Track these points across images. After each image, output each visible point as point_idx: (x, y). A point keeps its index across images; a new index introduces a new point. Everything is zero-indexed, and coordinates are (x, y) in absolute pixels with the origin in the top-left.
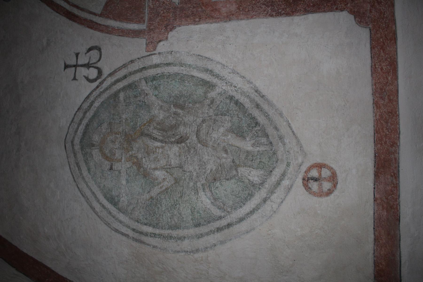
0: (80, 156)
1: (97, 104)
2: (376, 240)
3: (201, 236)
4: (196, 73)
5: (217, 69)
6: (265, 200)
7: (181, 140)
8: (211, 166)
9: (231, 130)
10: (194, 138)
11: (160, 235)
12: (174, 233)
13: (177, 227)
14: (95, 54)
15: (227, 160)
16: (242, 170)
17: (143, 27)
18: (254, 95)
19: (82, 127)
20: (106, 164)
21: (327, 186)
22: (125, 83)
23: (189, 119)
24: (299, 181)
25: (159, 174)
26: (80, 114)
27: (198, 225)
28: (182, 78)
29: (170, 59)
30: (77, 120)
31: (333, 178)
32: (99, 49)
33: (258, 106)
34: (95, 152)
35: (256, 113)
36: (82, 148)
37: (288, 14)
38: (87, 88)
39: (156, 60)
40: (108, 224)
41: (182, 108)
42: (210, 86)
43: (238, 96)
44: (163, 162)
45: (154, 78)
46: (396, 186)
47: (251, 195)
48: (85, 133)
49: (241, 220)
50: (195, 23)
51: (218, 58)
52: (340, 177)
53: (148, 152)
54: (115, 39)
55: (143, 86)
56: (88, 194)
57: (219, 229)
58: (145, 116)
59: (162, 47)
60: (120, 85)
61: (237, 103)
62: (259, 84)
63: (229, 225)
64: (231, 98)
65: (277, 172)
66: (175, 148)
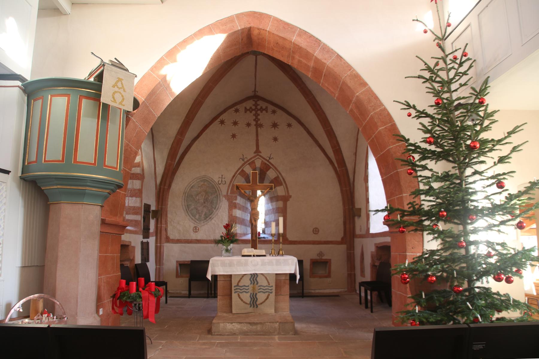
7: (204, 203)
8: (199, 209)
14: (224, 183)
15: (200, 212)
28: (217, 203)
31: (196, 232)
34: (202, 183)
39: (221, 197)
42: (215, 209)
53: (202, 195)
54: (227, 188)
59: (224, 199)
62: (215, 218)
66: (203, 201)
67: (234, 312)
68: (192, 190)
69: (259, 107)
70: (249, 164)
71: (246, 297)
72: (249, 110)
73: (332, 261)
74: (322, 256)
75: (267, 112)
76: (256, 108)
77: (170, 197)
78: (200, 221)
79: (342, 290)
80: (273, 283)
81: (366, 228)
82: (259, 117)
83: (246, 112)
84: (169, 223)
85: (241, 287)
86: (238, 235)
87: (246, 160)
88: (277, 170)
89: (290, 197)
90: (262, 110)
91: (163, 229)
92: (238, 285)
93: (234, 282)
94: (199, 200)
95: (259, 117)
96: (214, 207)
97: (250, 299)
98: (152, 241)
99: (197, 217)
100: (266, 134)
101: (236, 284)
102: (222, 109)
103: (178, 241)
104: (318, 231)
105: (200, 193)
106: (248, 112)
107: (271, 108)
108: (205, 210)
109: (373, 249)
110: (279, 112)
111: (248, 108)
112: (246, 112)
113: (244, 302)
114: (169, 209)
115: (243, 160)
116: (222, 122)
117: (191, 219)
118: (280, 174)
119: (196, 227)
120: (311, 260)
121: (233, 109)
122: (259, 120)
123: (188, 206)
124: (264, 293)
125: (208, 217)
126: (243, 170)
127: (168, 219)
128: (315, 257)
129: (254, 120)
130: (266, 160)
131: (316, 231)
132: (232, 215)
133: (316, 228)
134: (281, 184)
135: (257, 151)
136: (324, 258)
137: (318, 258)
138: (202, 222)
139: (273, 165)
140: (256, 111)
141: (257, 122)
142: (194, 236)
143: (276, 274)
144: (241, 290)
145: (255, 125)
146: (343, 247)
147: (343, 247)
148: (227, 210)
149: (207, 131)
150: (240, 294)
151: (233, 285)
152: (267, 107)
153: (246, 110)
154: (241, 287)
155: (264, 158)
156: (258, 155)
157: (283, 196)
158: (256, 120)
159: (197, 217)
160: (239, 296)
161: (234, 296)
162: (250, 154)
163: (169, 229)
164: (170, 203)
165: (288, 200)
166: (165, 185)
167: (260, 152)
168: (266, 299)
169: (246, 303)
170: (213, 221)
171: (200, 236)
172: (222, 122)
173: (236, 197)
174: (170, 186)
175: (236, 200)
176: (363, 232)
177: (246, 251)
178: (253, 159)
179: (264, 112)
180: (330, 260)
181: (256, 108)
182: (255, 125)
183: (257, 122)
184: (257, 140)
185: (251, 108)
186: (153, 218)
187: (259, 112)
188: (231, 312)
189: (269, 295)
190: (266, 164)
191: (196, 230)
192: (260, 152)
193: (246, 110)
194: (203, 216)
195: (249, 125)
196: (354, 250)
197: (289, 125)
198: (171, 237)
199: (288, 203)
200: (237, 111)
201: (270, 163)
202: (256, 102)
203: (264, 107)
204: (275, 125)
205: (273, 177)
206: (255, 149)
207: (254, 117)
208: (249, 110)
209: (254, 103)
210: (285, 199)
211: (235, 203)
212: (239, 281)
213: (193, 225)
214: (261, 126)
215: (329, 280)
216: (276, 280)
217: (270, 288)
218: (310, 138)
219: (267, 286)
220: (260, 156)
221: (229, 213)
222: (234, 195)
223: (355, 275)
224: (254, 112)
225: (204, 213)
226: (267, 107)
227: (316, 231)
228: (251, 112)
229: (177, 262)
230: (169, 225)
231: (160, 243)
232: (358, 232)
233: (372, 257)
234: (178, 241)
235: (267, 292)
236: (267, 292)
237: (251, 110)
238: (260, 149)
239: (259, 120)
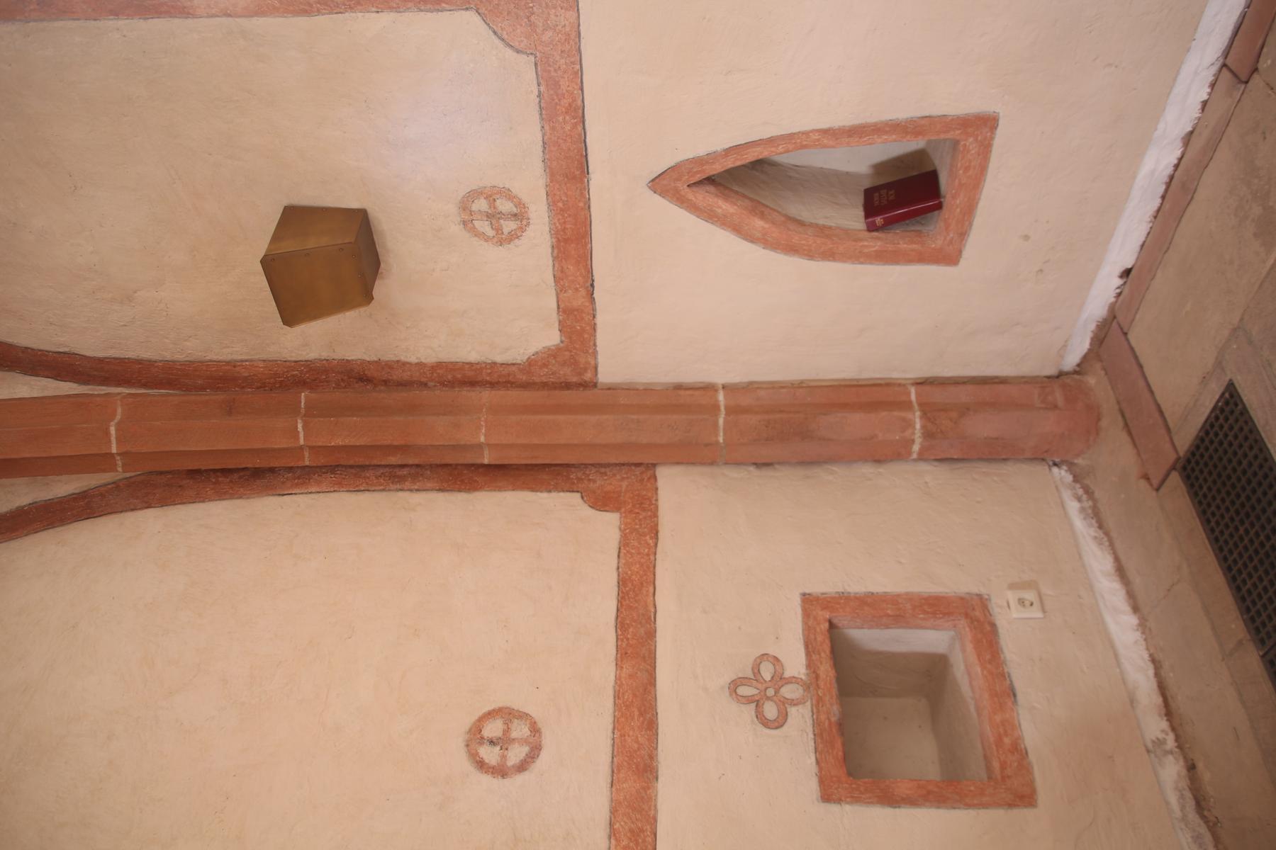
73: (826, 583)
74: (780, 680)
79: (1073, 506)
104: (507, 714)
120: (827, 796)
128: (794, 751)
131: (502, 742)
133: (475, 735)
136: (796, 664)
137: (801, 719)
146: (677, 490)
180: (809, 601)
215: (1012, 618)
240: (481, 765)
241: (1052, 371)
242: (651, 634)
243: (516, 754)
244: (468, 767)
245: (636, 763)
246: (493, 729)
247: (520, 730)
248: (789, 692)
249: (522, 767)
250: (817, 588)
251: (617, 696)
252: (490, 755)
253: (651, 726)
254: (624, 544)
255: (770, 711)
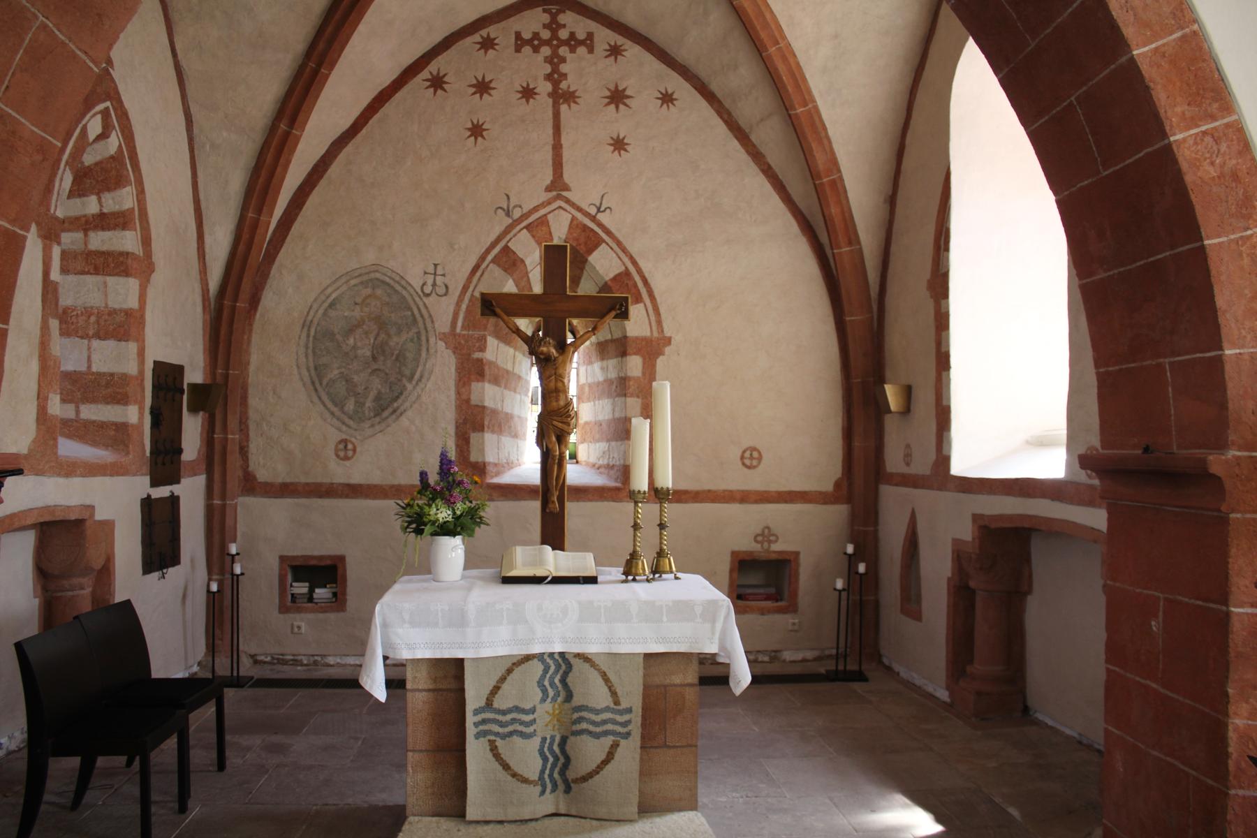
0: (365, 278)
1: (404, 293)
2: (307, 484)
3: (308, 370)
4: (420, 369)
5: (421, 385)
6: (332, 414)
7: (374, 358)
8: (356, 378)
9: (379, 393)
10: (376, 367)
11: (308, 340)
12: (310, 351)
13: (314, 352)
14: (442, 290)
15: (360, 389)
16: (352, 400)
17: (458, 330)
18: (402, 408)
19: (387, 280)
20: (359, 300)
21: (342, 454)
22: (418, 316)
23: (389, 363)
24: (344, 437)
25: (351, 341)
26: (397, 278)
27: (316, 369)
28: (417, 360)
29: (432, 351)
30: (394, 275)
31: (346, 458)
32: (445, 294)
33: (395, 411)
34: (369, 291)
35: (390, 410)
36: (371, 280)
37: (456, 434)
38: (417, 284)
39: (432, 340)
40: (315, 300)
41: (397, 359)
42: (411, 379)
43: (402, 397)
44: (359, 344)
45: (419, 339)
46: (341, 497)
47: (336, 405)
48: (383, 282)
49: (320, 398)
50: (457, 369)
51: (429, 385)
52: (347, 463)
54: (452, 309)
55: (415, 330)
56: (339, 283)
57: (313, 383)
58: (393, 331)
59: (441, 344)
60: (416, 312)
61: (398, 397)
62: (409, 413)
63: (316, 390)
64: (401, 394)
65: (351, 423)
66: (368, 354)
67: (471, 813)
68: (332, 313)
69: (564, 34)
70: (527, 227)
71: (527, 756)
72: (529, 42)
74: (770, 542)
75: (591, 50)
76: (555, 35)
77: (255, 338)
78: (361, 420)
80: (633, 698)
81: (934, 457)
82: (564, 68)
83: (518, 50)
84: (252, 426)
85: (504, 713)
86: (489, 468)
87: (517, 214)
88: (624, 250)
89: (668, 341)
90: (573, 42)
91: (233, 449)
92: (489, 704)
93: (474, 696)
94: (354, 348)
95: (564, 68)
96: (407, 372)
97: (540, 762)
98: (190, 492)
99: (350, 406)
100: (587, 129)
101: (483, 703)
102: (437, 38)
103: (285, 490)
104: (760, 458)
105: (358, 326)
106: (527, 50)
107: (605, 37)
108: (377, 384)
109: (966, 532)
110: (633, 51)
111: (527, 35)
112: (518, 50)
113: (514, 775)
114: (252, 379)
115: (508, 214)
116: (437, 83)
117: (327, 415)
118: (634, 263)
119: (345, 442)
120: (734, 554)
121: (477, 37)
122: (564, 76)
123: (319, 371)
124: (597, 736)
125: (386, 406)
126: (506, 249)
127: (252, 414)
128: (746, 544)
129: (549, 77)
130: (587, 214)
131: (751, 458)
132: (468, 401)
133: (753, 449)
134: (638, 299)
135: (558, 185)
136: (776, 547)
138: (367, 424)
139: (608, 233)
140: (555, 45)
141: (556, 84)
142: (339, 473)
143: (648, 657)
144: (502, 725)
145: (549, 95)
146: (839, 512)
147: (839, 512)
148: (452, 383)
149: (388, 109)
150: (499, 743)
151: (470, 707)
152: (590, 36)
153: (520, 43)
154: (504, 713)
155: (579, 209)
156: (559, 197)
157: (644, 339)
158: (555, 77)
159: (350, 406)
160: (494, 749)
161: (476, 751)
162: (530, 191)
163: (253, 448)
164: (255, 359)
165: (660, 353)
166: (236, 298)
167: (567, 189)
168: (606, 762)
169: (525, 781)
170: (404, 421)
171: (359, 471)
172: (437, 83)
173: (483, 340)
174: (255, 301)
175: (483, 349)
176: (922, 465)
177: (523, 560)
178: (542, 212)
179: (582, 50)
180: (797, 554)
181: (555, 35)
182: (549, 95)
183: (556, 84)
184: (557, 148)
185: (536, 35)
186: (193, 409)
187: (563, 51)
188: (459, 813)
189: (615, 746)
190: (585, 228)
191: (345, 450)
192: (567, 189)
193: (520, 43)
194: (369, 404)
195: (528, 93)
196: (876, 523)
197: (667, 99)
198: (262, 475)
199: (660, 362)
200: (488, 44)
201: (600, 225)
202: (554, 17)
203: (581, 35)
204: (617, 97)
205: (612, 275)
206: (548, 178)
207: (548, 69)
208: (529, 42)
209: (546, 18)
210: (652, 349)
211: (480, 361)
212: (496, 689)
213: (334, 436)
214: (570, 97)
216: (647, 688)
217: (619, 718)
218: (736, 143)
219: (607, 709)
220: (568, 201)
221: (458, 393)
222: (477, 333)
223: (877, 604)
224: (546, 51)
225: (372, 395)
226: (590, 36)
227: (751, 458)
228: (536, 50)
229: (283, 559)
230: (252, 434)
231: (223, 497)
232: (894, 461)
233: (959, 556)
234: (285, 490)
235: (606, 733)
236: (606, 733)
237: (535, 43)
238: (567, 176)
239: (564, 76)
240: (744, 452)
241: (882, 652)
242: (786, 502)
243: (748, 462)
244: (745, 446)
245: (744, 497)
246: (755, 454)
247: (755, 463)
248: (766, 545)
249: (744, 464)
250: (802, 556)
251: (766, 492)
252: (747, 454)
253: (756, 502)
254: (821, 493)
255: (760, 538)
